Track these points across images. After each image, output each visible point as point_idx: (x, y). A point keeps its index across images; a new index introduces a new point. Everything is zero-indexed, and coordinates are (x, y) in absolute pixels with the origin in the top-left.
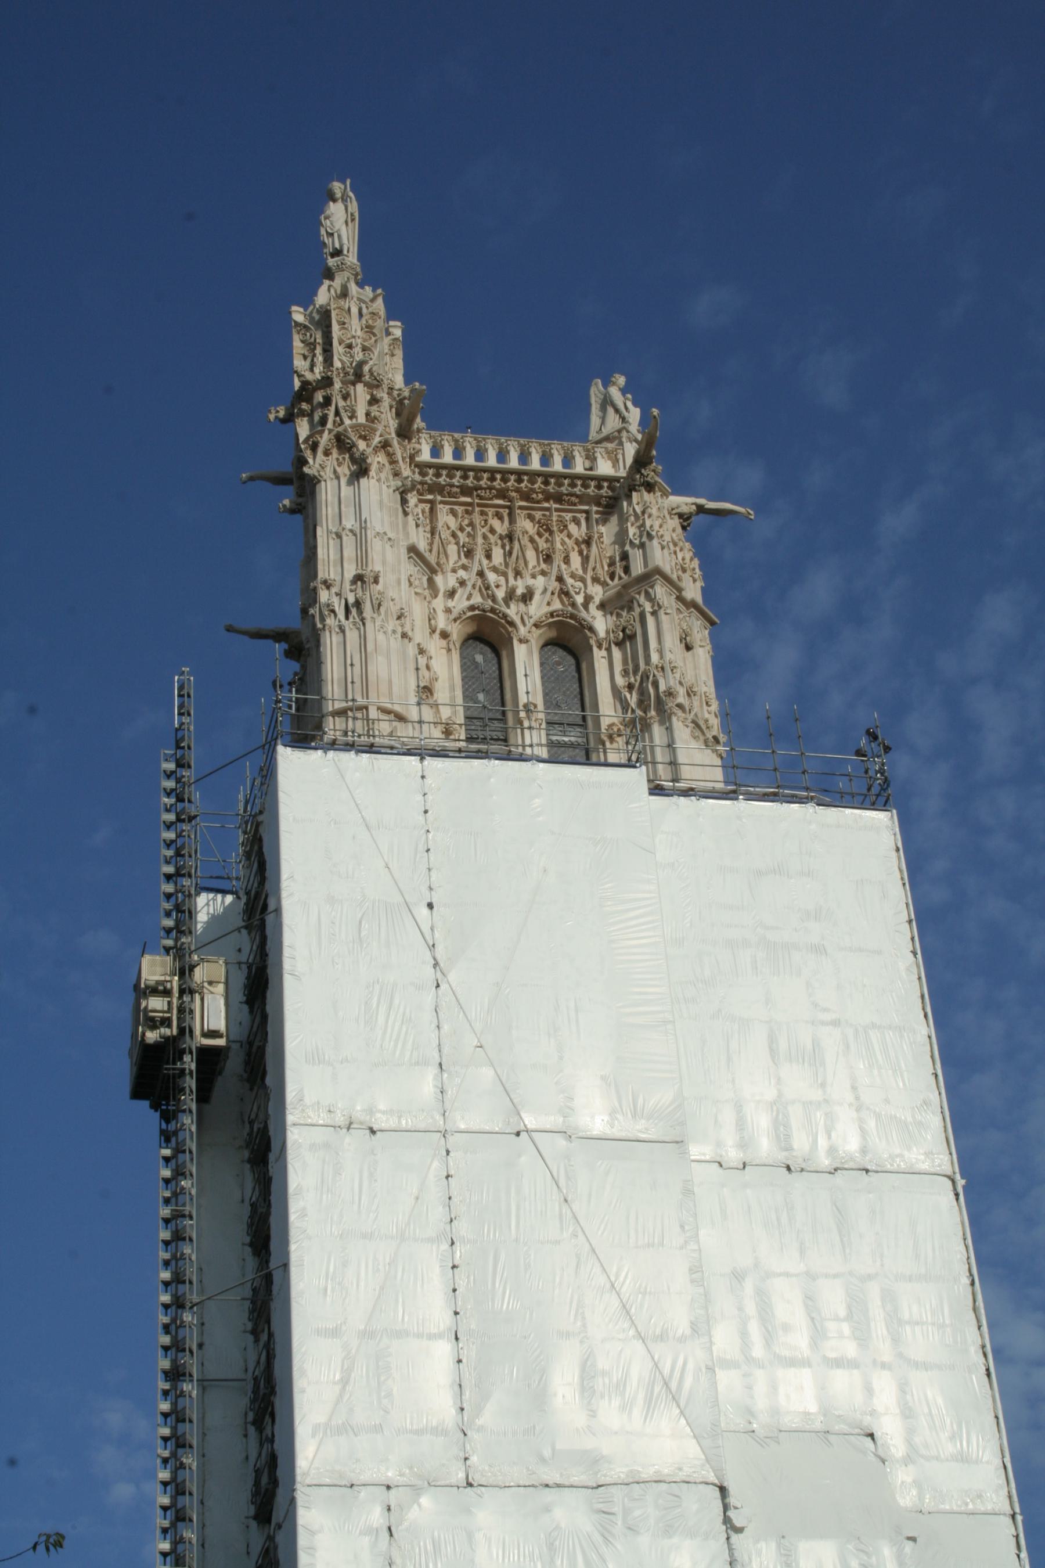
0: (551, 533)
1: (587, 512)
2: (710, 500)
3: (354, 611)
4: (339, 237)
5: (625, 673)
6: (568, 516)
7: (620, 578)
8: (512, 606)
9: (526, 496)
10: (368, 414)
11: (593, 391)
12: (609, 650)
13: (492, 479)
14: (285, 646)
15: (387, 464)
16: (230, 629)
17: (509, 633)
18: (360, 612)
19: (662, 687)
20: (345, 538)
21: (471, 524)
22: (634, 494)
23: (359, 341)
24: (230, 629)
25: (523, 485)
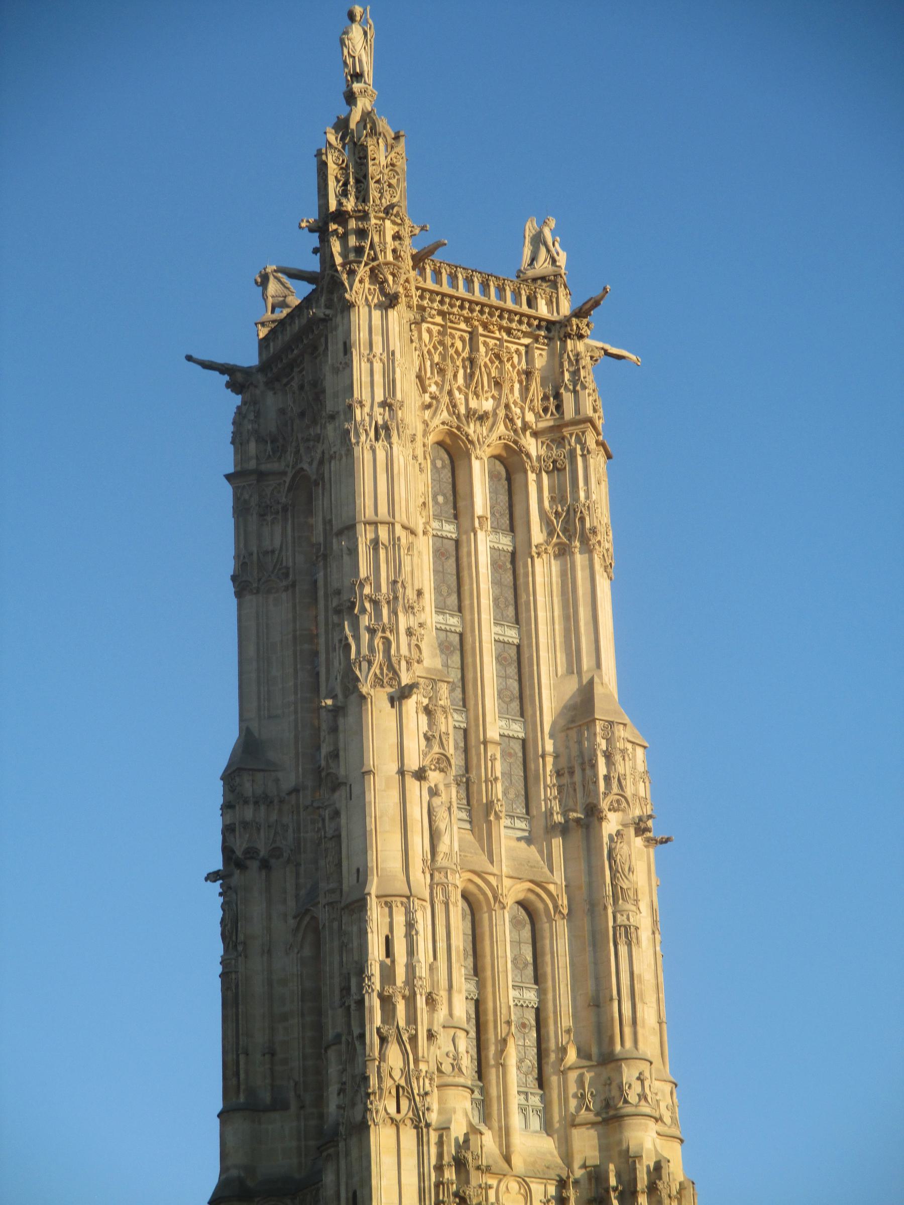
0: (501, 362)
1: (527, 346)
2: (613, 345)
3: (383, 433)
4: (360, 61)
5: (552, 499)
6: (513, 347)
7: (552, 414)
8: (472, 425)
9: (485, 326)
10: (394, 251)
11: (528, 224)
12: (539, 475)
16: (189, 358)
17: (468, 450)
18: (388, 437)
19: (588, 525)
20: (375, 364)
21: (441, 343)
22: (569, 341)
23: (386, 177)
24: (189, 358)
25: (485, 317)
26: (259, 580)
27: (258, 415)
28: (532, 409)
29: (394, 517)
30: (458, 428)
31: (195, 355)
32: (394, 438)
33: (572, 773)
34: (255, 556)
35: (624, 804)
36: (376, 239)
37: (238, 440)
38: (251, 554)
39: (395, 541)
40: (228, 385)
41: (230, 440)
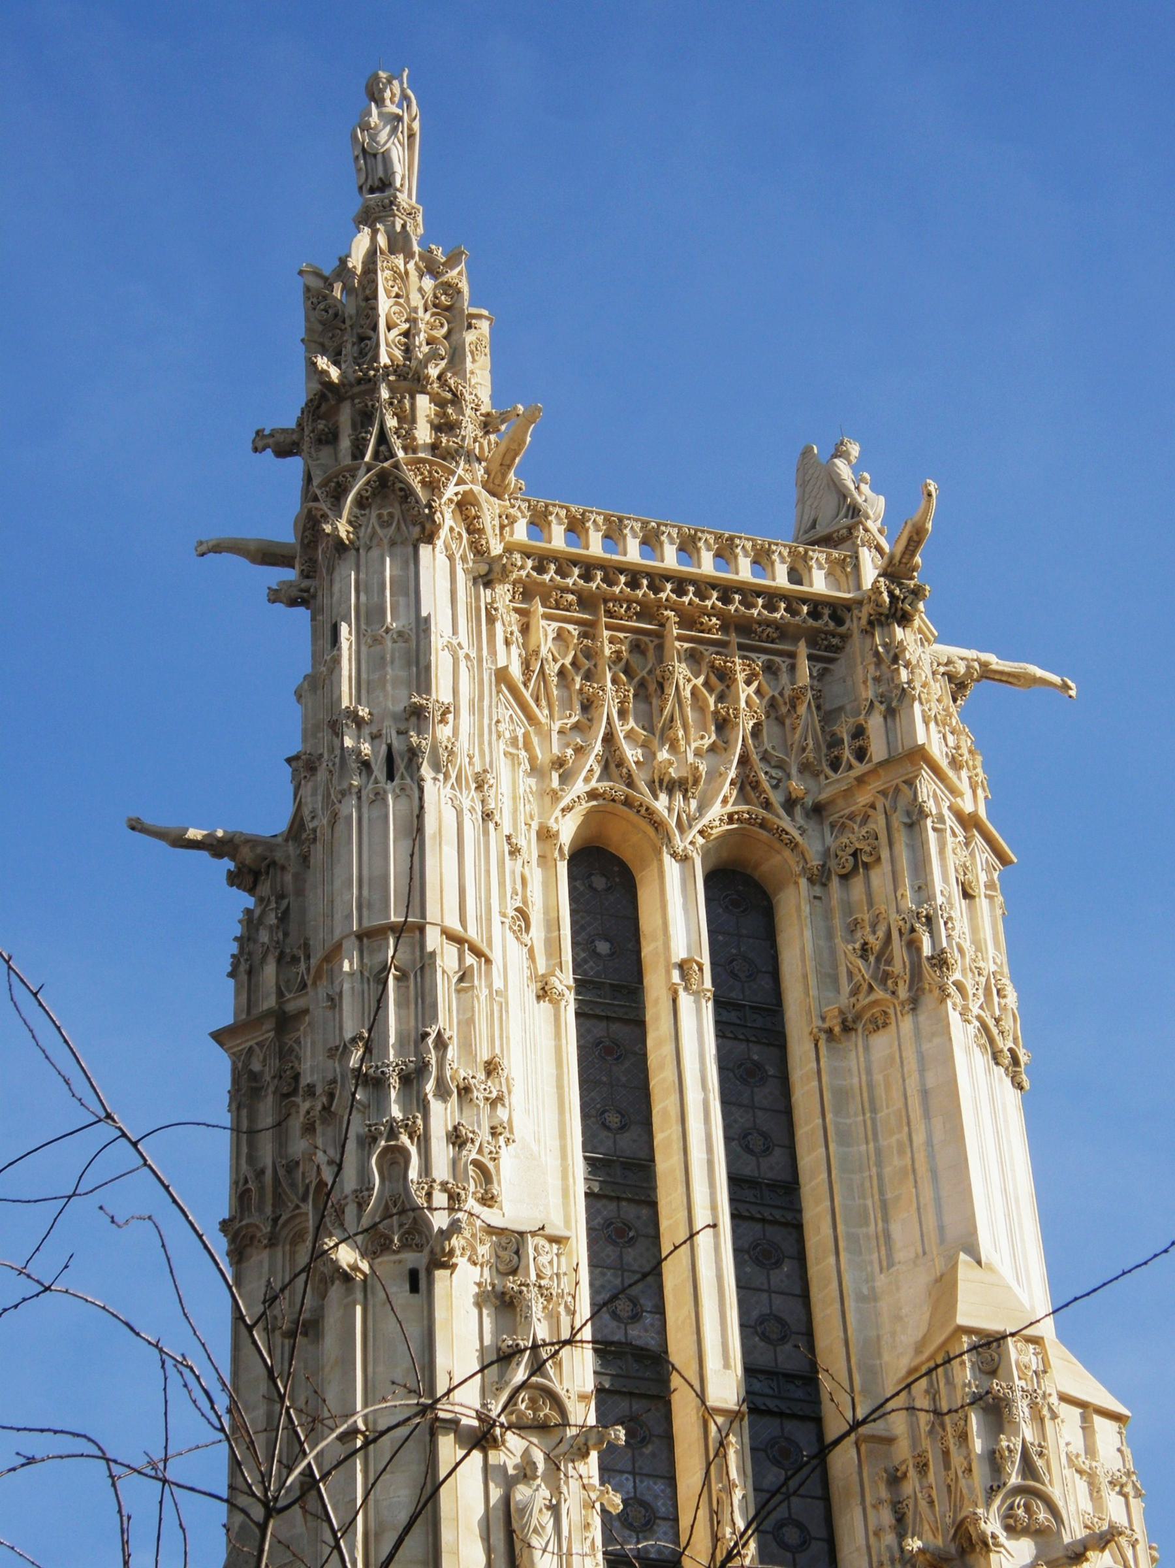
3: (400, 765)
13: (634, 584)
14: (228, 864)
15: (465, 535)
16: (136, 826)
19: (927, 950)
24: (136, 826)
26: (275, 1220)
27: (284, 918)
28: (805, 768)
29: (423, 916)
30: (627, 802)
31: (149, 820)
32: (426, 771)
33: (922, 1468)
34: (269, 1172)
35: (1042, 1515)
36: (391, 422)
37: (244, 967)
38: (260, 1173)
39: (425, 964)
40: (234, 879)
41: (229, 969)
